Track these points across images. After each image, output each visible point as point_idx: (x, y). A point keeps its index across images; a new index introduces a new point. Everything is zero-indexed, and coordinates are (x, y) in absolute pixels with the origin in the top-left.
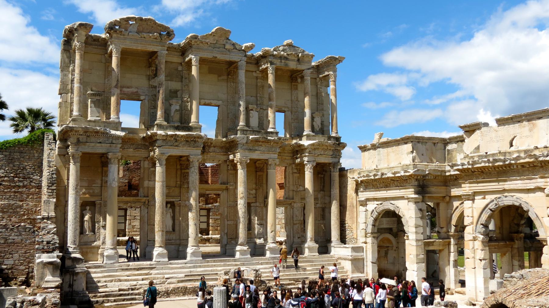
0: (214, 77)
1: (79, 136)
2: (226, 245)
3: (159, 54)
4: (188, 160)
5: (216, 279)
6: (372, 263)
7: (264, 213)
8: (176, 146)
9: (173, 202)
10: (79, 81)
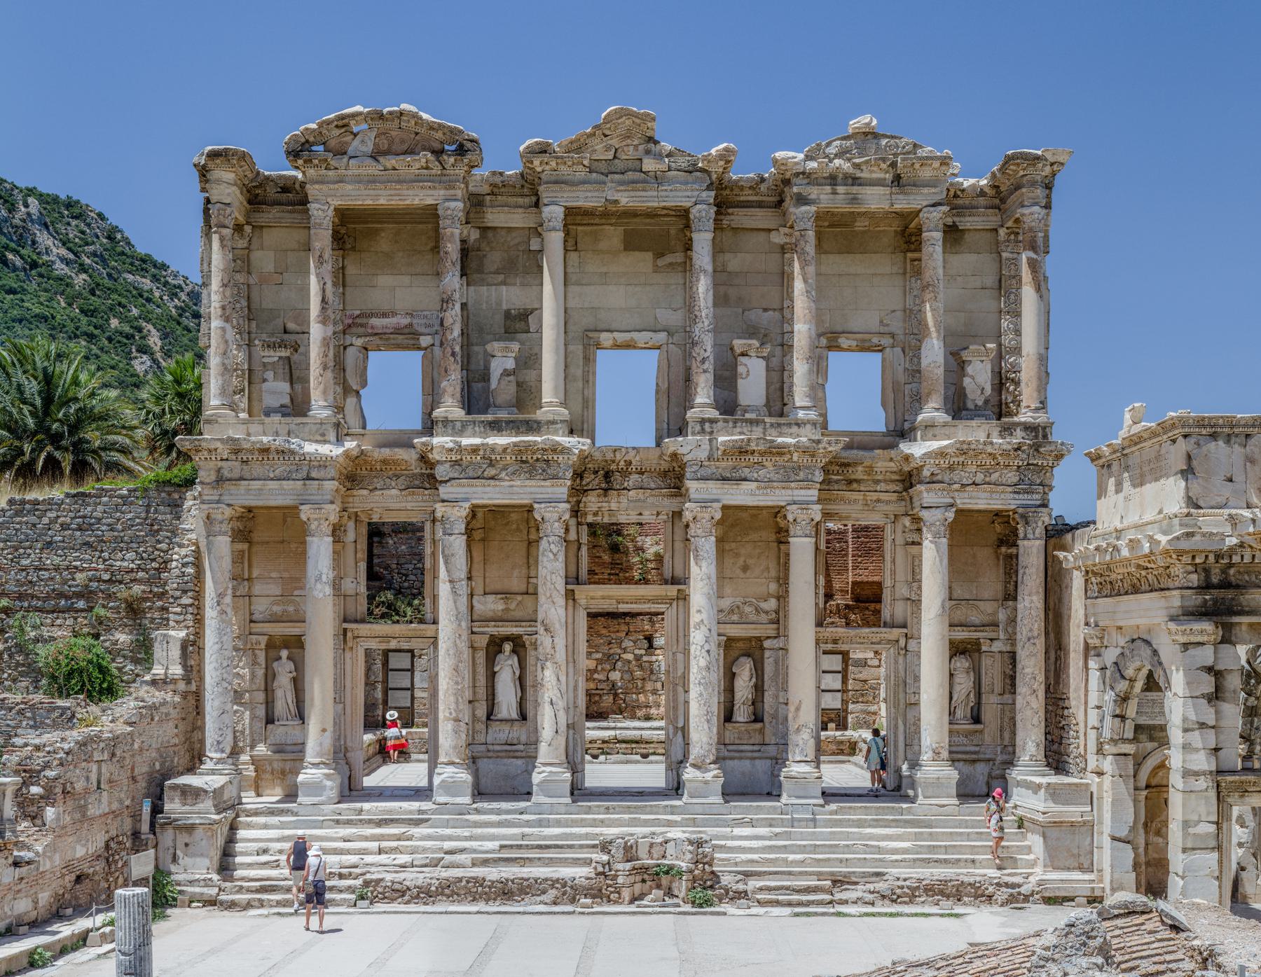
1: (220, 464)
2: (681, 762)
5: (588, 862)
6: (1114, 839)
8: (492, 478)
9: (520, 636)
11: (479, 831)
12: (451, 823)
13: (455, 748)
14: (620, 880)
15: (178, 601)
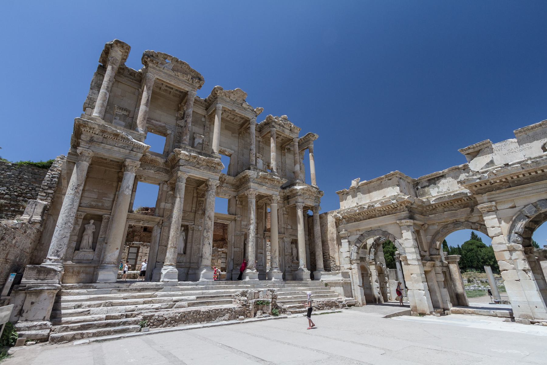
0: (229, 133)
3: (189, 93)
4: (207, 185)
5: (231, 302)
7: (264, 243)
10: (106, 88)
11: (184, 292)
12: (172, 290)
13: (173, 259)
14: (251, 307)
15: (46, 191)
